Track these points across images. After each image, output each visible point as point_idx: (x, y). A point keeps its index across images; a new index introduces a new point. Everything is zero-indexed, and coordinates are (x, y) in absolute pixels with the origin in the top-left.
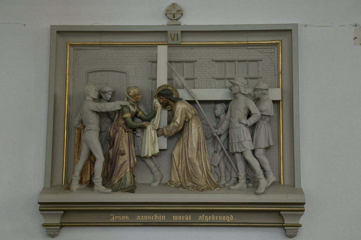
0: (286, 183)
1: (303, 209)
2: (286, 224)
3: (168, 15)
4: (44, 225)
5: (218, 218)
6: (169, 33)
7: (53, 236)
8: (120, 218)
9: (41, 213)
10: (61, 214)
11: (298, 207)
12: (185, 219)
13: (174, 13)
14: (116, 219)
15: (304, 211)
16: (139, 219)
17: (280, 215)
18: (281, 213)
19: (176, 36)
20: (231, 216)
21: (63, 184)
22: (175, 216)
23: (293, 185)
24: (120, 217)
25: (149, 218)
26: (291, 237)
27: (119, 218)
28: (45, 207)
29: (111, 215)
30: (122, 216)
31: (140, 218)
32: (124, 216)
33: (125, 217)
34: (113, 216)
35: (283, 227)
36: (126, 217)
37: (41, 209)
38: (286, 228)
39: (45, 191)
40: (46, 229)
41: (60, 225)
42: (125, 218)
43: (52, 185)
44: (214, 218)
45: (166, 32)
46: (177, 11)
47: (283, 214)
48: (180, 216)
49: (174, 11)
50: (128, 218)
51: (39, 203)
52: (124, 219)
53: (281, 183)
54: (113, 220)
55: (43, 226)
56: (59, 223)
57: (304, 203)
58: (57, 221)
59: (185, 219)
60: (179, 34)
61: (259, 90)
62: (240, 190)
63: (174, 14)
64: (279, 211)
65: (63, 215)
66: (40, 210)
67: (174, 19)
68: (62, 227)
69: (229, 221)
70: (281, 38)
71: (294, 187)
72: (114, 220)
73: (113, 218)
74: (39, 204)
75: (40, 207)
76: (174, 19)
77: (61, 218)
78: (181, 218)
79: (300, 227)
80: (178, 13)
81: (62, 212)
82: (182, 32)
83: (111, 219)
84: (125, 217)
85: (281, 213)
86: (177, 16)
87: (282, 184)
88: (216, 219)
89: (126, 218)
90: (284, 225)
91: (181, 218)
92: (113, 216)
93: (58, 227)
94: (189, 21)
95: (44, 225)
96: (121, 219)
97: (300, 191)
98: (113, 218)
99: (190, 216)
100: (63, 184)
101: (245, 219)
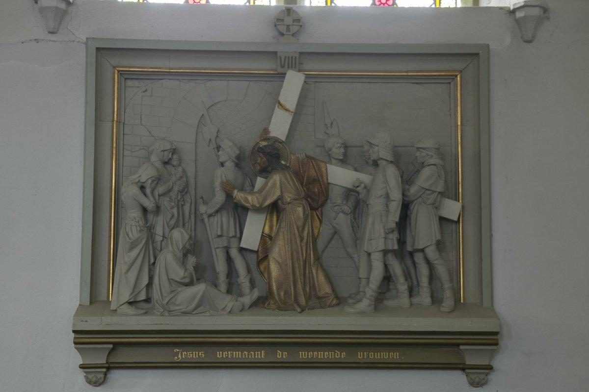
2: (467, 365)
4: (82, 367)
5: (368, 354)
6: (279, 55)
7: (97, 384)
9: (76, 348)
10: (107, 350)
11: (490, 340)
14: (183, 357)
16: (247, 357)
18: (461, 347)
20: (336, 351)
22: (237, 353)
23: (483, 302)
24: (190, 354)
26: (474, 384)
28: (83, 338)
30: (194, 353)
31: (248, 355)
33: (199, 353)
35: (463, 369)
36: (200, 353)
37: (76, 340)
38: (467, 371)
41: (107, 365)
44: (281, 355)
45: (275, 53)
46: (294, 21)
47: (465, 350)
49: (288, 21)
50: (203, 355)
52: (197, 357)
53: (460, 301)
54: (178, 358)
56: (105, 362)
58: (102, 360)
60: (297, 56)
61: (422, 150)
62: (362, 313)
63: (288, 26)
64: (458, 345)
65: (112, 350)
66: (75, 343)
67: (289, 33)
68: (109, 367)
72: (180, 358)
73: (180, 356)
74: (73, 334)
75: (75, 338)
76: (289, 33)
80: (294, 24)
81: (111, 346)
82: (301, 53)
83: (176, 358)
84: (199, 353)
86: (294, 29)
87: (462, 302)
88: (224, 357)
89: (200, 355)
90: (465, 366)
92: (179, 352)
93: (104, 370)
95: (82, 367)
96: (193, 356)
97: (491, 312)
98: (180, 356)
99: (263, 352)
101: (415, 356)
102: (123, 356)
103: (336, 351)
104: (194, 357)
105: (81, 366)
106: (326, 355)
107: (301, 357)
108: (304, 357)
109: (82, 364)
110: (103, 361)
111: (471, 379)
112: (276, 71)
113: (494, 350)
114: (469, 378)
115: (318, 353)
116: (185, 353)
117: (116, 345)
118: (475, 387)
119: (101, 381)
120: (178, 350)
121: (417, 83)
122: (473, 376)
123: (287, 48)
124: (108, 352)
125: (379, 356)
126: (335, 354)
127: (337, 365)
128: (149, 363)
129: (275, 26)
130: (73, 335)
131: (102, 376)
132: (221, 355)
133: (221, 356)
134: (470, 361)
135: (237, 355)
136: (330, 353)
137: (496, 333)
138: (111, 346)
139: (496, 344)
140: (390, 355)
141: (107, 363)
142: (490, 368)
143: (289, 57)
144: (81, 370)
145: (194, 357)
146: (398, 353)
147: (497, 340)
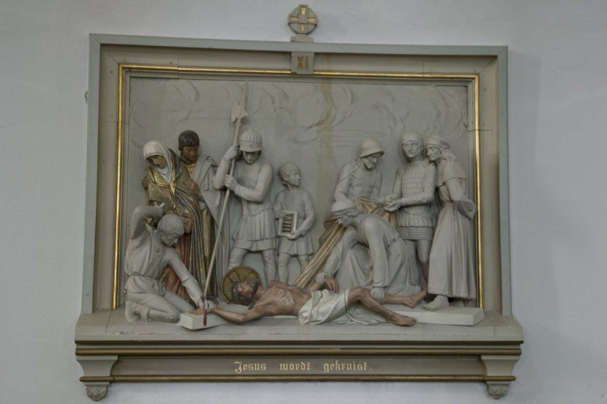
3: (295, 27)
4: (83, 380)
6: (293, 55)
8: (252, 367)
10: (115, 360)
12: (345, 369)
13: (303, 22)
14: (244, 369)
15: (519, 354)
17: (481, 362)
18: (484, 358)
24: (251, 366)
26: (497, 396)
27: (249, 367)
28: (86, 349)
29: (235, 363)
30: (255, 365)
32: (258, 365)
34: (238, 365)
35: (484, 381)
37: (81, 352)
41: (111, 378)
42: (260, 368)
43: (95, 309)
48: (292, 364)
50: (265, 368)
51: (77, 342)
52: (259, 369)
54: (239, 371)
55: (81, 380)
56: (109, 375)
57: (522, 342)
58: (105, 372)
59: (345, 369)
64: (479, 356)
65: (117, 362)
66: (77, 354)
68: (112, 381)
70: (479, 70)
71: (502, 313)
73: (240, 369)
75: (77, 349)
78: (290, 367)
79: (512, 382)
81: (116, 358)
82: (316, 54)
83: (236, 370)
85: (484, 358)
89: (262, 367)
90: (486, 378)
91: (290, 367)
92: (239, 364)
93: (108, 383)
94: (324, 39)
95: (83, 380)
96: (254, 368)
97: (511, 320)
98: (240, 369)
102: (128, 370)
103: (302, 363)
104: (256, 369)
105: (82, 379)
106: (331, 367)
108: (284, 369)
109: (81, 378)
112: (290, 70)
113: (517, 361)
116: (246, 365)
117: (120, 355)
119: (103, 395)
120: (238, 363)
121: (453, 86)
124: (111, 366)
125: (351, 367)
126: (300, 366)
127: (350, 377)
129: (289, 24)
130: (75, 346)
132: (286, 367)
134: (491, 372)
135: (284, 366)
137: (522, 342)
138: (116, 358)
141: (111, 375)
142: (513, 379)
144: (82, 383)
147: (519, 349)
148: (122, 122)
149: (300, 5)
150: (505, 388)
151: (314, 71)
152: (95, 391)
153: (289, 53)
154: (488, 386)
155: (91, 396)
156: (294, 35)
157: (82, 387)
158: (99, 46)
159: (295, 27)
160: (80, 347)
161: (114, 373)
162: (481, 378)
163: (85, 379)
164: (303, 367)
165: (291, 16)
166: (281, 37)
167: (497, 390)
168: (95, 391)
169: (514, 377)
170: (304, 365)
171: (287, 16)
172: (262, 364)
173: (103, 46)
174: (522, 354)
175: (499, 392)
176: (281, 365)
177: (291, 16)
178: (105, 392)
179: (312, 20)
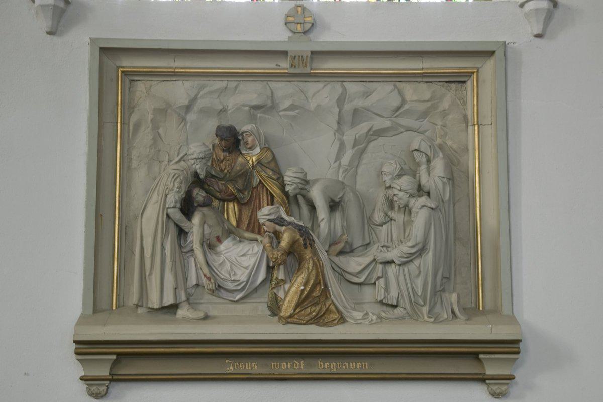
0: (488, 307)
1: (516, 350)
3: (293, 27)
4: (82, 379)
6: (289, 55)
9: (77, 359)
10: (114, 360)
11: (510, 347)
18: (481, 356)
19: (303, 59)
21: (114, 308)
24: (242, 365)
25: (253, 366)
27: (241, 366)
28: (86, 348)
30: (247, 364)
32: (250, 364)
33: (251, 365)
34: (231, 363)
36: (253, 364)
37: (80, 351)
38: (488, 382)
39: (83, 320)
40: (87, 385)
41: (111, 377)
43: (95, 311)
50: (256, 366)
51: (75, 342)
52: (250, 368)
54: (230, 370)
56: (108, 374)
58: (105, 372)
60: (309, 54)
66: (77, 353)
69: (335, 370)
73: (231, 368)
75: (76, 349)
77: (111, 369)
79: (513, 381)
81: (114, 357)
82: (312, 53)
85: (481, 356)
87: (481, 309)
93: (107, 383)
95: (82, 379)
97: (512, 320)
100: (114, 308)
104: (247, 368)
107: (273, 368)
110: (105, 372)
111: (492, 389)
113: (517, 359)
114: (490, 389)
115: (362, 364)
116: (237, 364)
117: (118, 354)
118: (496, 398)
119: (103, 393)
120: (229, 361)
122: (495, 388)
123: (303, 47)
128: (211, 374)
129: (286, 23)
131: (105, 388)
133: (279, 368)
134: (490, 371)
135: (276, 366)
136: (363, 364)
138: (114, 357)
139: (518, 353)
140: (358, 365)
141: (110, 374)
142: (511, 378)
143: (299, 56)
145: (247, 368)
146: (367, 364)
147: (519, 348)
148: (121, 123)
149: (296, 5)
150: (504, 388)
151: (311, 70)
152: (94, 389)
153: (285, 53)
154: (488, 385)
155: (91, 394)
156: (290, 34)
157: (83, 386)
158: (99, 48)
159: (293, 27)
160: (78, 346)
161: (113, 372)
162: (481, 377)
163: (86, 378)
164: (297, 366)
165: (287, 16)
166: (277, 35)
167: (496, 389)
168: (94, 389)
169: (513, 376)
170: (298, 364)
171: (284, 16)
172: (254, 363)
173: (103, 50)
174: (521, 352)
175: (499, 391)
176: (273, 364)
177: (288, 16)
178: (105, 391)
179: (307, 19)
